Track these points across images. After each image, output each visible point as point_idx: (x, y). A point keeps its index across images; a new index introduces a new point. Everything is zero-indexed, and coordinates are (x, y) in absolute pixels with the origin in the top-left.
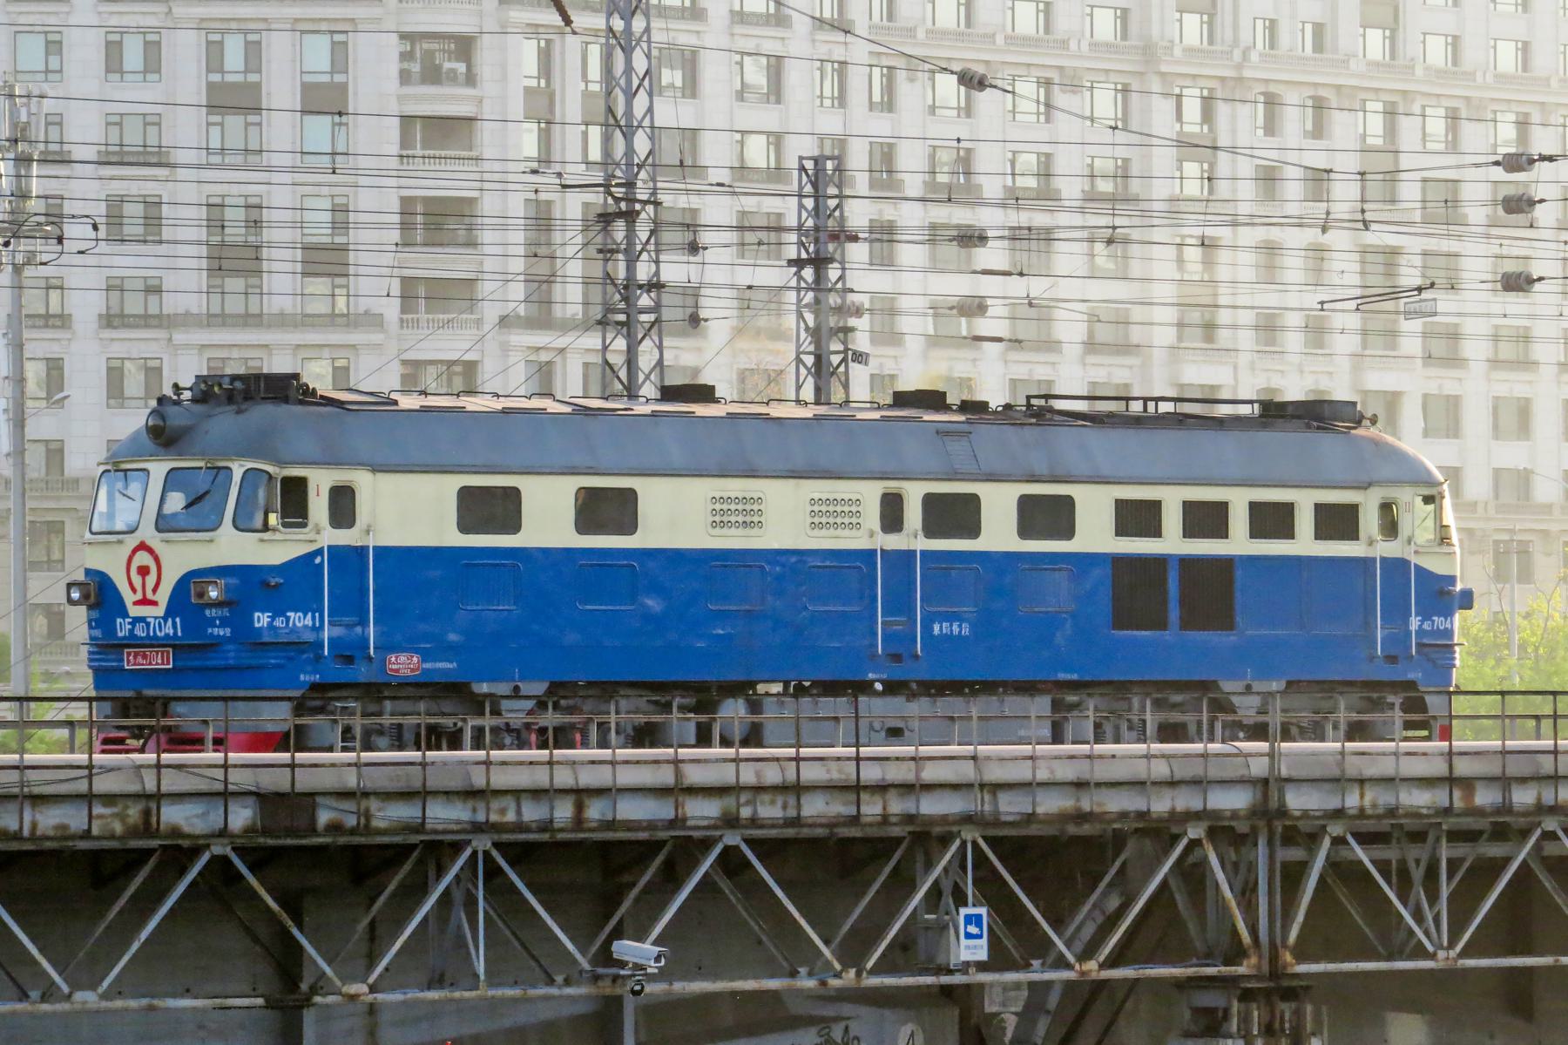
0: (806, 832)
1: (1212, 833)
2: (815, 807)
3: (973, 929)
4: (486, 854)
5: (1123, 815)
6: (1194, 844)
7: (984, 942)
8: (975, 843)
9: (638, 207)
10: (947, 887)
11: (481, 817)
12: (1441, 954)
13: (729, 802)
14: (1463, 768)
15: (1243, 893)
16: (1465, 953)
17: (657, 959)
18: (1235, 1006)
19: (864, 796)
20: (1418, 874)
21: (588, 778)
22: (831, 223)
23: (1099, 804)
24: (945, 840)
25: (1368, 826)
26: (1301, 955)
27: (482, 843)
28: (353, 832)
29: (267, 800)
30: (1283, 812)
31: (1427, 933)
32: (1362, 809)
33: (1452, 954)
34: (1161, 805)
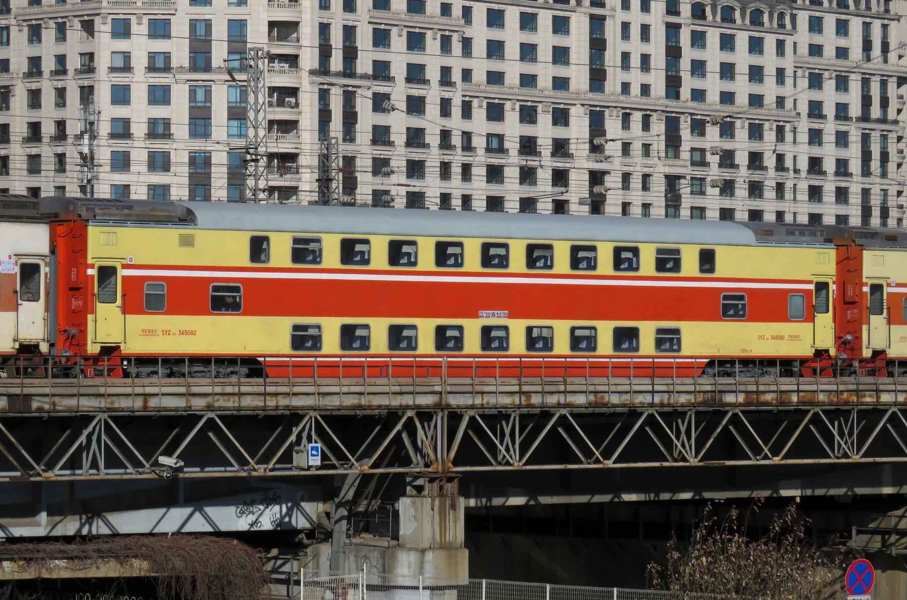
0: (243, 413)
1: (418, 414)
2: (247, 402)
3: (314, 453)
4: (105, 421)
5: (380, 407)
6: (410, 419)
7: (319, 458)
8: (316, 418)
9: (259, 157)
10: (305, 435)
11: (103, 405)
12: (516, 464)
13: (210, 399)
14: (525, 388)
15: (432, 438)
16: (524, 465)
17: (176, 464)
18: (427, 485)
19: (267, 398)
20: (507, 431)
21: (149, 390)
22: (334, 164)
23: (369, 402)
24: (303, 416)
25: (487, 412)
26: (456, 463)
27: (105, 416)
28: (49, 412)
29: (9, 396)
30: (448, 406)
31: (511, 457)
32: (482, 405)
33: (521, 464)
34: (396, 402)
